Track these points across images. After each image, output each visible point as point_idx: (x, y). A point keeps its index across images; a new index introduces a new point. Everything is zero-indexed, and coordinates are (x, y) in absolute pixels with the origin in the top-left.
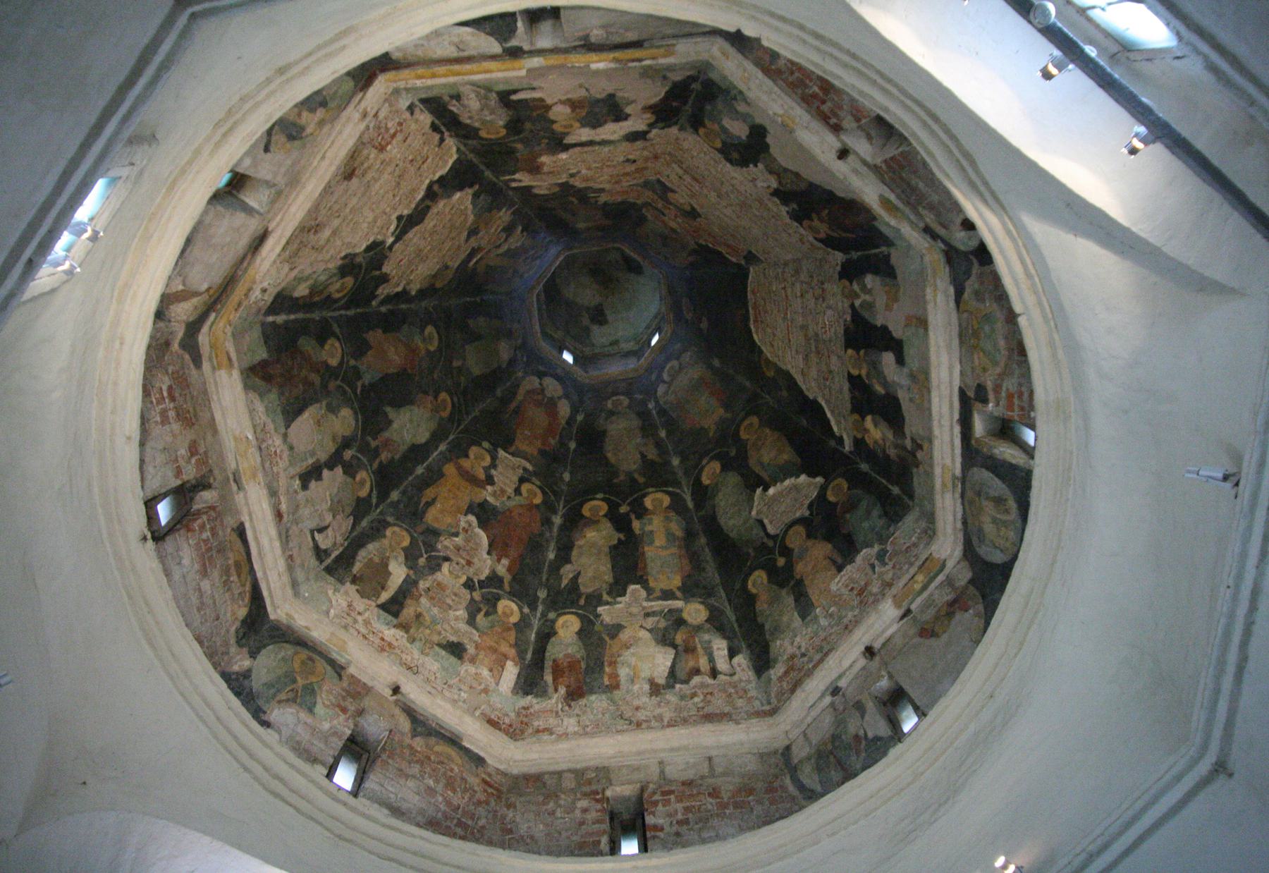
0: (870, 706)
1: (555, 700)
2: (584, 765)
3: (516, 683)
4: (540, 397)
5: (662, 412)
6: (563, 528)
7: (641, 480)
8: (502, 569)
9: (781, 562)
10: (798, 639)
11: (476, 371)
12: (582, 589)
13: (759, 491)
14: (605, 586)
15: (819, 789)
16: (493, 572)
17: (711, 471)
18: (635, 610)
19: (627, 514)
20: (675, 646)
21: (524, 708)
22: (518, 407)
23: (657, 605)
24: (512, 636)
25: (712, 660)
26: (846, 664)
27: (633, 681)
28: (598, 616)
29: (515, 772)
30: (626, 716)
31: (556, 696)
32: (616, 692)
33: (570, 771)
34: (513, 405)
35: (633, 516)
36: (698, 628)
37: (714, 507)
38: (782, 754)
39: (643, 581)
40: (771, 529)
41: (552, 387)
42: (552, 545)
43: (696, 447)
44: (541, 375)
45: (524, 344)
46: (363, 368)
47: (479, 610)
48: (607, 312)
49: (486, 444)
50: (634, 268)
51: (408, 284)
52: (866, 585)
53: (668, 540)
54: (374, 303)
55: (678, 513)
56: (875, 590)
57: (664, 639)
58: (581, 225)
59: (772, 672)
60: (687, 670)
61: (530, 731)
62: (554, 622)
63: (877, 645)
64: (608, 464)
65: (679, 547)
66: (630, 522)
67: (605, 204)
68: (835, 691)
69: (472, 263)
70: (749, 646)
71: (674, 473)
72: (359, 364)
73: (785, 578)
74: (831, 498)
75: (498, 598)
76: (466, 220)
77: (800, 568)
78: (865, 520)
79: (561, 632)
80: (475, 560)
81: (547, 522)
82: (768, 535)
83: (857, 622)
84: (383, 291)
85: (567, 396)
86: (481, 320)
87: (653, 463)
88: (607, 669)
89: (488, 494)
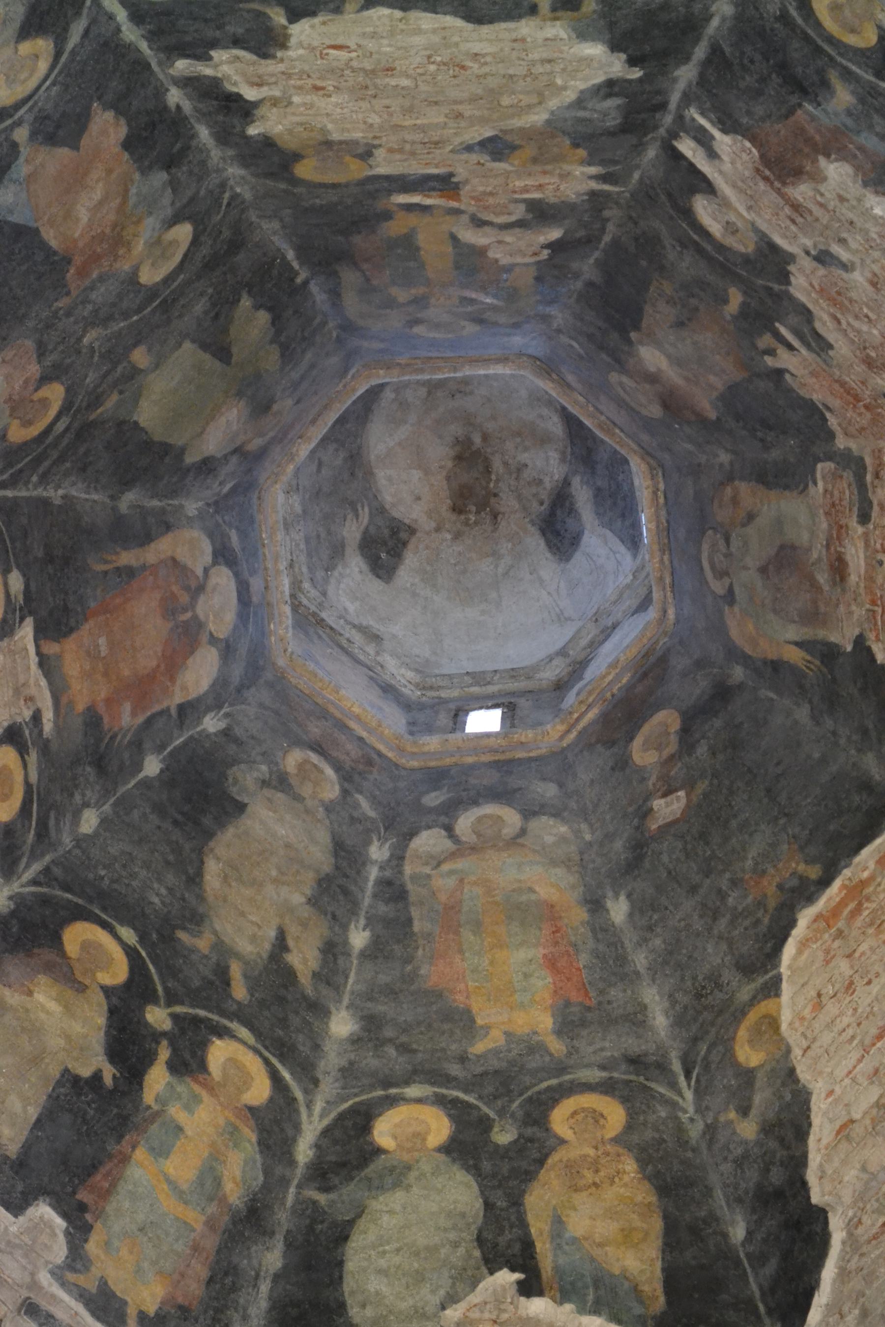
4: (184, 598)
5: (393, 891)
7: (240, 992)
11: (148, 415)
13: (506, 1278)
17: (412, 1125)
19: (157, 1036)
22: (130, 573)
34: (127, 558)
35: (164, 1053)
43: (417, 1039)
44: (223, 555)
45: (261, 454)
46: (21, 169)
48: (411, 560)
50: (558, 531)
51: (275, 102)
53: (200, 1181)
54: (182, 66)
55: (264, 1145)
58: (650, 357)
64: (195, 879)
65: (210, 1223)
66: (149, 1059)
67: (779, 373)
69: (402, 199)
71: (317, 1047)
72: (24, 151)
76: (521, 110)
84: (229, 66)
85: (227, 650)
86: (263, 317)
87: (289, 975)
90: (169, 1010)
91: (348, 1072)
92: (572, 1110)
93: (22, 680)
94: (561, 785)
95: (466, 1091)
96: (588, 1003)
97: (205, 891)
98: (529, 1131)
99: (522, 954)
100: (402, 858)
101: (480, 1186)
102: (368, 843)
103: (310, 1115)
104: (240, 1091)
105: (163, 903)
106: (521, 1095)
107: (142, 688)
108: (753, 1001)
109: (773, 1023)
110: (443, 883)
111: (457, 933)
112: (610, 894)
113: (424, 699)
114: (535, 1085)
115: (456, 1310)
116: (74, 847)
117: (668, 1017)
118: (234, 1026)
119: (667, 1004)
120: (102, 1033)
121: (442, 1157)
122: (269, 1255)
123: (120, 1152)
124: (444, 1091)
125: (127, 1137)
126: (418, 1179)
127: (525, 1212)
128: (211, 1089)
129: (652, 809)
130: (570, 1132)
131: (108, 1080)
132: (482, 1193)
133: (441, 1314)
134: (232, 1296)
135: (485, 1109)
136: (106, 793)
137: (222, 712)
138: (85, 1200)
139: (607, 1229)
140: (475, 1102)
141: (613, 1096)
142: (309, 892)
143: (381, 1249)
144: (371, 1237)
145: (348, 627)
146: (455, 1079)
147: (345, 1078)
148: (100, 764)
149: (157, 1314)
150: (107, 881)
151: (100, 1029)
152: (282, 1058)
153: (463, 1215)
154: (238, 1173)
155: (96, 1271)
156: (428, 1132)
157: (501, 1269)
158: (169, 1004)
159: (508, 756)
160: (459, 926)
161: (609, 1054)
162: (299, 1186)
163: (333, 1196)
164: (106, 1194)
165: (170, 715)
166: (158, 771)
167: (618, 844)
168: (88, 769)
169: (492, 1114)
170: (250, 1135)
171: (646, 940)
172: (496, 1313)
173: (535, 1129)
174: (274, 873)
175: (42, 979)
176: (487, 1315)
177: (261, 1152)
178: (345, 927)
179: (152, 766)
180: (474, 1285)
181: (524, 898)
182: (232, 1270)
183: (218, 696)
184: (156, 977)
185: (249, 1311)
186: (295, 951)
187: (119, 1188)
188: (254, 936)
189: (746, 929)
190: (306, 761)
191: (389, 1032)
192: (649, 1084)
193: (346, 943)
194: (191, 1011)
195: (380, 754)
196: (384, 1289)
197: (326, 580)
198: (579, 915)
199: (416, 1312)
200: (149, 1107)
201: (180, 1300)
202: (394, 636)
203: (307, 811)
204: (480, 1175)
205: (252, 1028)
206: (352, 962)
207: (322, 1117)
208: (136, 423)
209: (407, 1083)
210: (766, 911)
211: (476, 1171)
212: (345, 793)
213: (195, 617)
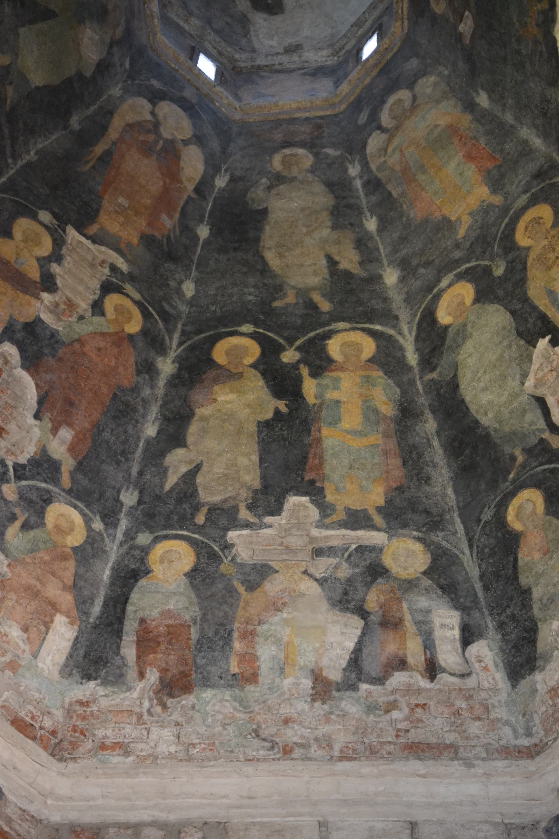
1: (139, 692)
2: (182, 815)
3: (70, 656)
4: (151, 137)
5: (374, 184)
6: (176, 381)
7: (325, 306)
8: (60, 446)
11: (37, 79)
12: (204, 496)
14: (244, 494)
16: (44, 451)
17: (455, 300)
18: (296, 541)
19: (295, 366)
20: (363, 614)
21: (81, 703)
22: (108, 153)
23: (338, 536)
24: (69, 569)
25: (429, 644)
27: (282, 671)
28: (227, 547)
29: (56, 818)
30: (265, 733)
31: (141, 685)
32: (250, 688)
33: (154, 824)
35: (305, 371)
36: (410, 585)
37: (455, 366)
39: (314, 490)
41: (175, 122)
42: (154, 410)
44: (155, 97)
45: (129, 32)
47: (13, 518)
49: (45, 216)
53: (366, 418)
55: (388, 373)
57: (346, 600)
59: (538, 677)
60: (383, 659)
61: (89, 745)
62: (146, 550)
64: (265, 270)
65: (386, 435)
66: (299, 380)
70: (501, 626)
71: (385, 300)
75: (48, 501)
79: (158, 570)
80: (12, 427)
81: (148, 369)
85: (198, 139)
87: (347, 274)
88: (237, 645)
89: (42, 308)
90: (294, 347)
91: (409, 300)
92: (524, 228)
93: (89, 257)
94: (417, 55)
95: (469, 261)
96: (498, 163)
97: (274, 271)
98: (510, 257)
99: (452, 165)
100: (367, 163)
101: (503, 306)
102: (346, 170)
103: (404, 337)
104: (358, 357)
105: (255, 296)
106: (495, 241)
107: (164, 200)
110: (393, 160)
111: (415, 180)
112: (474, 94)
113: (341, 58)
114: (499, 229)
115: (530, 380)
116: (190, 308)
117: (540, 138)
118: (334, 326)
119: (535, 131)
120: (266, 389)
121: (478, 305)
122: (427, 425)
123: (314, 439)
124: (459, 270)
125: (313, 429)
126: (473, 327)
127: (533, 302)
128: (342, 368)
129: (461, 33)
130: (530, 240)
131: (284, 409)
132: (506, 308)
133: (524, 388)
134: (421, 461)
135: (483, 263)
136: (188, 269)
137: (223, 171)
138: (311, 478)
140: (476, 263)
141: (540, 203)
142: (329, 224)
143: (477, 378)
144: (469, 376)
145: (275, 58)
146: (460, 259)
147: (408, 303)
148: (171, 257)
149: (386, 502)
150: (218, 311)
151: (263, 387)
152: (370, 321)
153: (504, 328)
154: (384, 398)
155: (340, 508)
156: (463, 299)
157: (538, 341)
158: (291, 344)
159: (384, 62)
160: (414, 176)
161: (524, 182)
162: (421, 378)
163: (438, 370)
165: (193, 199)
166: (208, 231)
167: (461, 64)
168: (166, 265)
169: (487, 263)
170: (378, 374)
171: (504, 105)
172: (549, 365)
173: (512, 253)
174: (304, 230)
175: (216, 388)
176: (546, 370)
177: (389, 377)
178: (361, 225)
179: (203, 232)
180: (530, 360)
181: (436, 134)
182: (414, 447)
183: (213, 167)
184: (276, 337)
185: (435, 460)
186: (342, 260)
187: (325, 457)
188: (315, 271)
189: (539, 61)
190: (285, 156)
191: (415, 262)
192: (552, 181)
193: (367, 232)
194: (305, 338)
195: (322, 118)
196: (491, 397)
197: (250, 41)
198: (468, 117)
199: (512, 396)
200: (314, 405)
201: (394, 485)
202: (307, 37)
203: (302, 182)
204: (500, 301)
205: (344, 320)
206: (376, 240)
207: (410, 333)
208: (37, 88)
209: (439, 281)
210: (541, 44)
211: (497, 300)
212: (316, 155)
213: (166, 141)
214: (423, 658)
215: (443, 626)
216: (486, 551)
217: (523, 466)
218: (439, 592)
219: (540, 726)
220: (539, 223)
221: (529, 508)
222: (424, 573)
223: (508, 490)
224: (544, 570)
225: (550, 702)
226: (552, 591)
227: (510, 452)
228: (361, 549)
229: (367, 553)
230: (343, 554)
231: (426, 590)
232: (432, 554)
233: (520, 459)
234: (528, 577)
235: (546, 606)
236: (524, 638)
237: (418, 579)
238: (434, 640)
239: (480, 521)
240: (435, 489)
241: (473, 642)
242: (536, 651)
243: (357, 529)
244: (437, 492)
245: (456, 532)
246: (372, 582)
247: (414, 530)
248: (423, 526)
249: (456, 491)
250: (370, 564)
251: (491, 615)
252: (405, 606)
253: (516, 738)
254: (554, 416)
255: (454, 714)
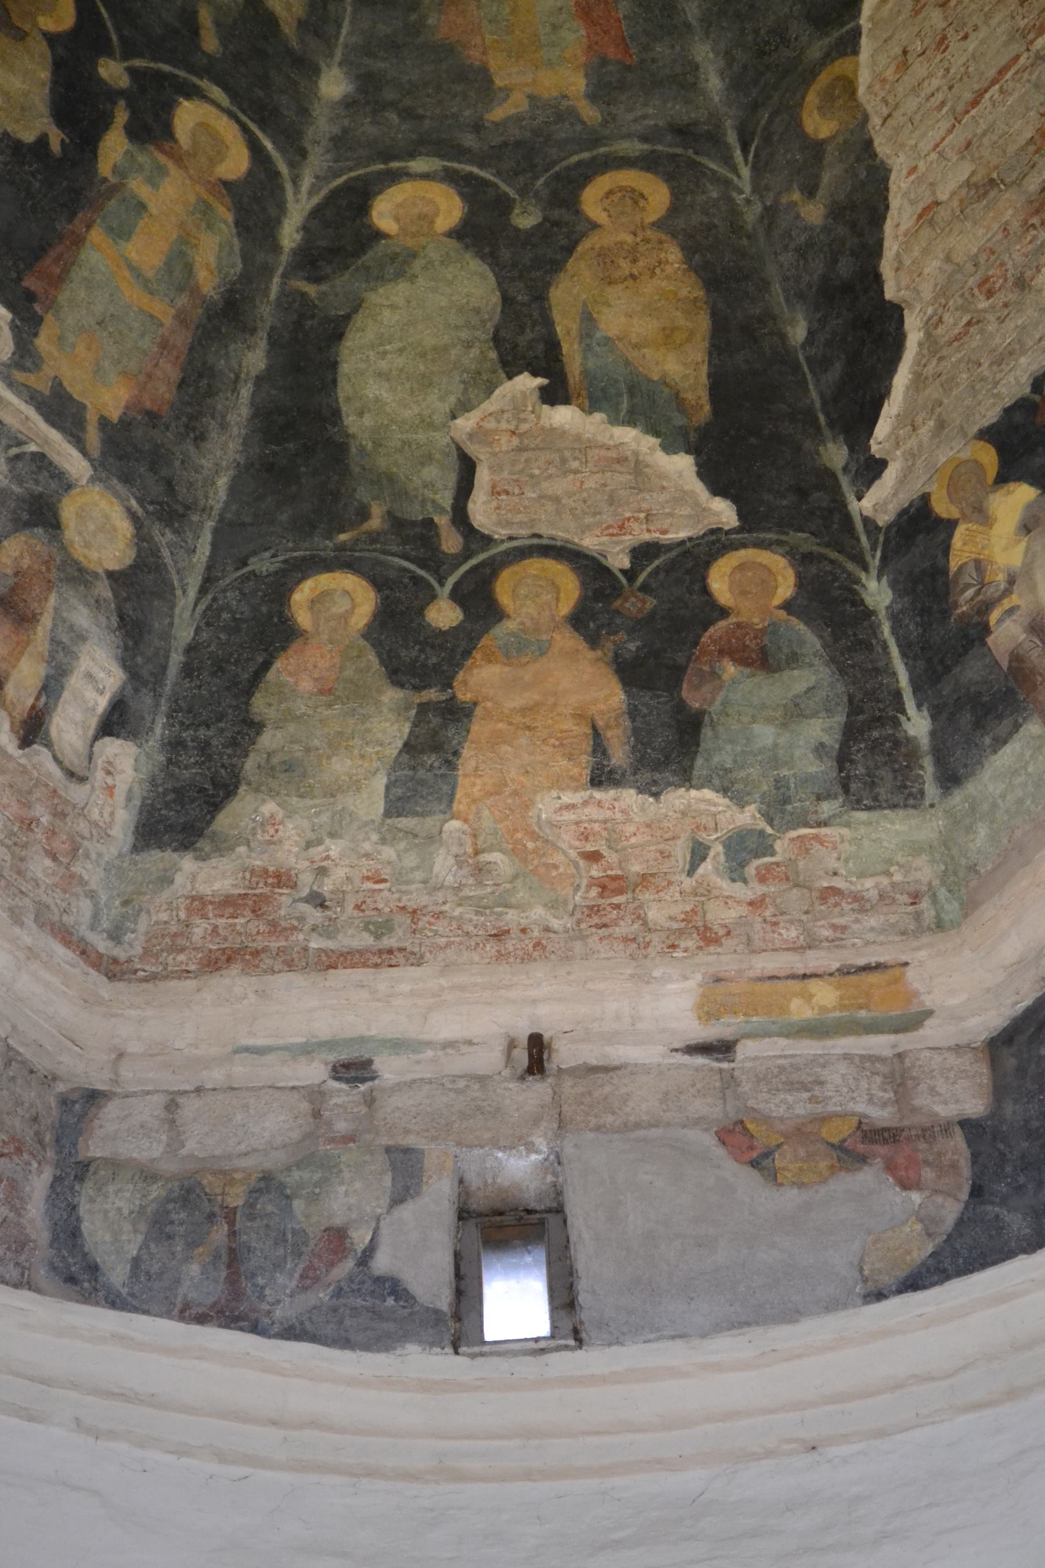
0: (438, 1196)
7: (210, 43)
9: (443, 614)
10: (335, 848)
13: (527, 383)
15: (117, 1275)
17: (416, 206)
19: (112, 95)
25: (52, 687)
26: (445, 1026)
35: (122, 116)
36: (78, 575)
38: (65, 1102)
40: (481, 511)
52: (645, 879)
53: (169, 266)
55: (242, 226)
56: (653, 914)
59: (187, 863)
63: (564, 1054)
65: (181, 317)
66: (104, 123)
68: (354, 1070)
70: (174, 745)
71: (304, 112)
73: (418, 659)
74: (720, 581)
77: (481, 678)
78: (775, 719)
82: (460, 517)
83: (538, 948)
90: (125, 64)
91: (340, 143)
92: (606, 189)
95: (481, 166)
98: (556, 214)
104: (213, 162)
106: (546, 171)
108: (827, 59)
109: (849, 86)
114: (564, 159)
115: (468, 419)
117: (723, 79)
118: (205, 84)
121: (453, 243)
122: (250, 355)
123: (73, 232)
124: (456, 165)
125: (80, 215)
126: (425, 268)
127: (550, 308)
128: (179, 160)
130: (604, 215)
131: (55, 147)
132: (499, 284)
133: (451, 423)
134: (208, 400)
135: (504, 187)
138: (33, 288)
139: (645, 327)
140: (492, 178)
141: (656, 173)
143: (381, 349)
144: (370, 335)
146: (469, 150)
149: (121, 420)
151: (44, 84)
152: (262, 124)
153: (477, 311)
154: (212, 260)
155: (48, 371)
156: (437, 214)
157: (520, 373)
158: (126, 56)
162: (284, 276)
163: (324, 287)
164: (58, 281)
169: (512, 193)
170: (225, 215)
172: (514, 423)
176: (504, 425)
177: (239, 235)
180: (489, 391)
185: (229, 418)
187: (73, 275)
192: (699, 159)
194: (152, 65)
196: (385, 395)
199: (423, 421)
200: (105, 180)
201: (148, 405)
205: (226, 88)
207: (311, 193)
209: (412, 155)
214: (30, 701)
215: (89, 676)
216: (225, 616)
217: (374, 538)
218: (114, 620)
219: (143, 938)
220: (636, 202)
221: (341, 606)
222: (110, 574)
223: (322, 553)
224: (304, 714)
225: (183, 915)
226: (299, 754)
227: (365, 501)
228: (40, 459)
229: (46, 474)
230: (9, 447)
231: (97, 601)
232: (138, 556)
233: (375, 523)
234: (270, 705)
235: (272, 768)
236: (202, 790)
237: (96, 575)
238: (63, 687)
239: (245, 564)
240: (203, 462)
241: (118, 737)
242: (209, 823)
243: (53, 424)
244: (202, 467)
245: (194, 551)
246: (28, 525)
247: (136, 498)
248: (152, 503)
249: (233, 489)
250: (41, 495)
251: (169, 716)
252: (53, 600)
253: (92, 928)
254: (475, 503)
255: (22, 822)
